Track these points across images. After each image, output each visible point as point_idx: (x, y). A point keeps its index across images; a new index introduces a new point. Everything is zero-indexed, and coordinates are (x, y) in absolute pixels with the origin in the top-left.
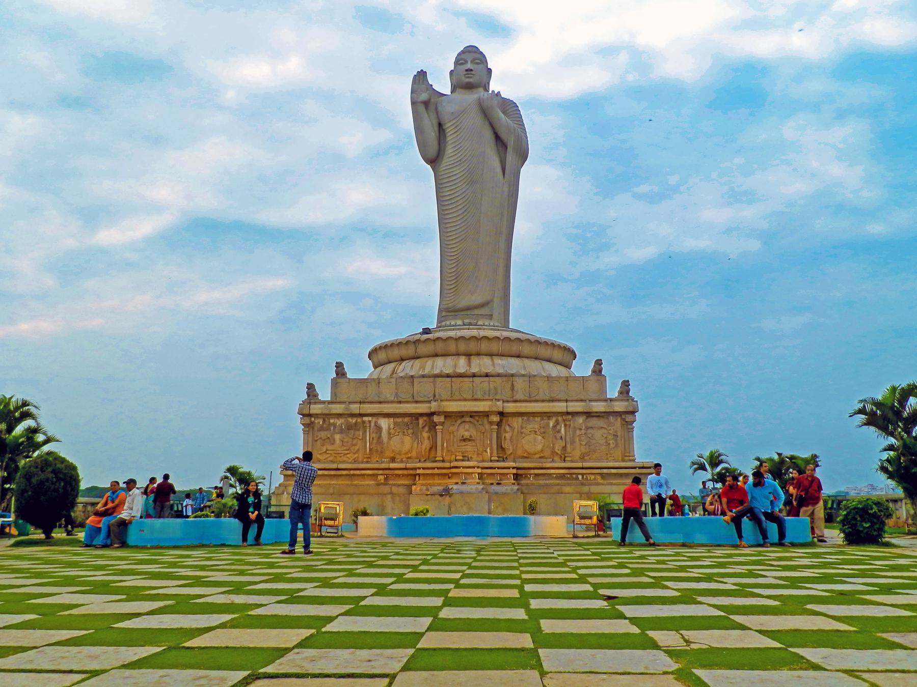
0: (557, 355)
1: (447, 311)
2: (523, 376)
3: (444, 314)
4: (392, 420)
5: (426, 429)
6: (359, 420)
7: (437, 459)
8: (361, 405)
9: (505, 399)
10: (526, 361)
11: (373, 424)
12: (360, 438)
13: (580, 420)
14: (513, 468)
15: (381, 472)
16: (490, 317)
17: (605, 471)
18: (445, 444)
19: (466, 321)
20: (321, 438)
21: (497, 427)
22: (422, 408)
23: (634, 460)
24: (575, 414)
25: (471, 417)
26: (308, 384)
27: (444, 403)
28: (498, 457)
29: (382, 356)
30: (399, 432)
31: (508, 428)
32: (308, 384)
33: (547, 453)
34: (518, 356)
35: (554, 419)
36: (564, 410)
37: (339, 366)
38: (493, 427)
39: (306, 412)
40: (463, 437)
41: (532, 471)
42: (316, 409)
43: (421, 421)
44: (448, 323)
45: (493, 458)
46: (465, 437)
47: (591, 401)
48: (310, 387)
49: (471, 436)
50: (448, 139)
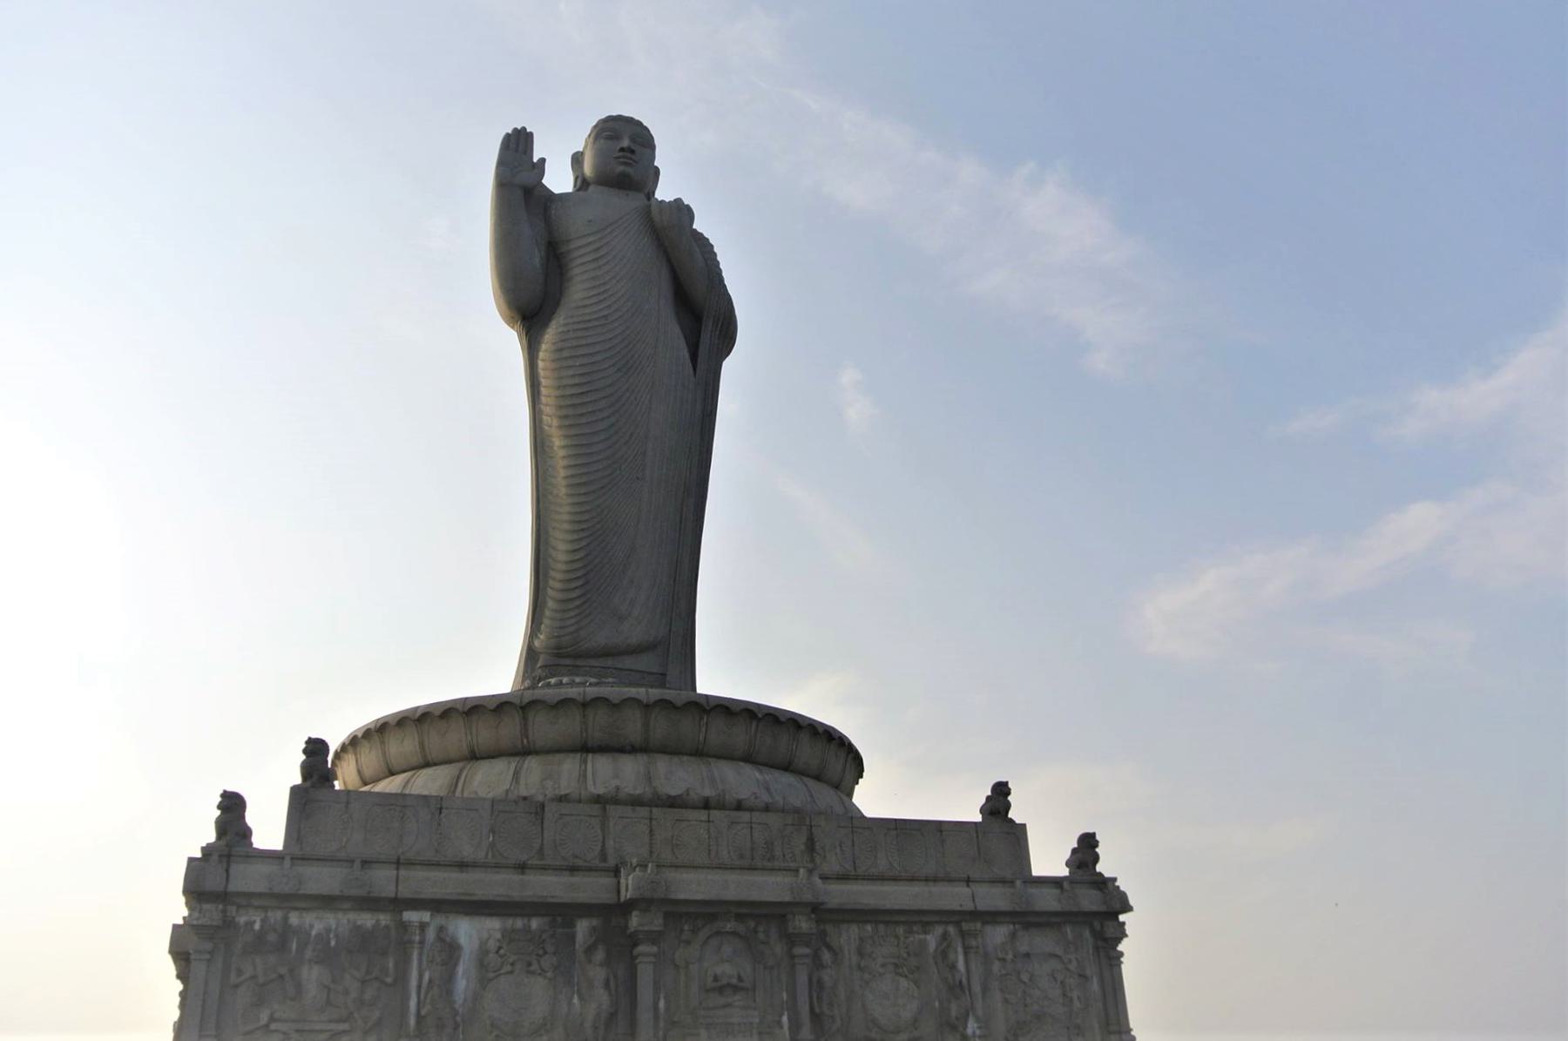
5: (600, 955)
8: (403, 872)
11: (431, 934)
12: (389, 980)
13: (997, 935)
20: (254, 977)
21: (807, 951)
22: (593, 889)
24: (992, 917)
27: (671, 875)
30: (512, 964)
31: (826, 956)
35: (939, 930)
36: (969, 906)
38: (799, 950)
39: (213, 883)
40: (716, 979)
42: (245, 879)
43: (583, 927)
46: (724, 981)
48: (232, 805)
50: (577, 271)
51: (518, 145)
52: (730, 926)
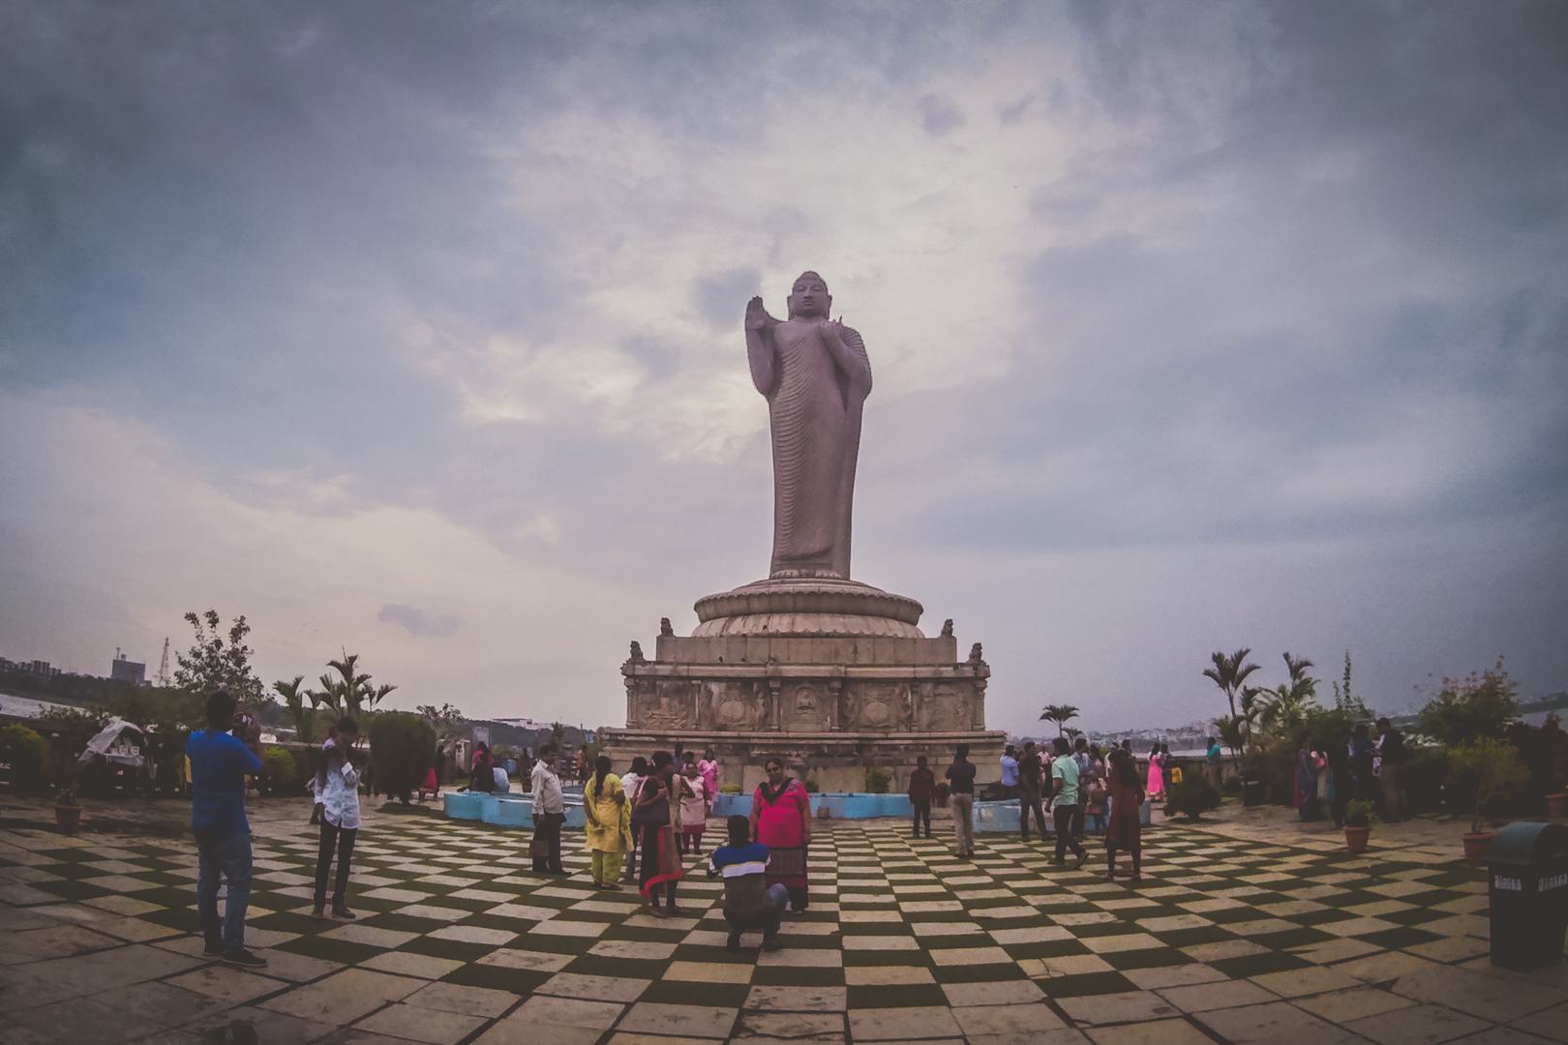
0: (904, 611)
1: (783, 560)
2: (868, 636)
3: (778, 562)
4: (724, 685)
7: (774, 727)
9: (848, 663)
10: (871, 620)
14: (856, 739)
16: (829, 567)
19: (804, 571)
22: (757, 672)
23: (983, 729)
24: (925, 680)
25: (811, 682)
26: (632, 642)
28: (839, 726)
29: (710, 610)
32: (632, 642)
33: (893, 721)
35: (901, 685)
37: (665, 622)
41: (876, 742)
42: (640, 670)
43: (755, 687)
44: (783, 572)
45: (833, 728)
47: (940, 665)
48: (635, 646)
49: (810, 704)
51: (756, 304)
52: (806, 685)
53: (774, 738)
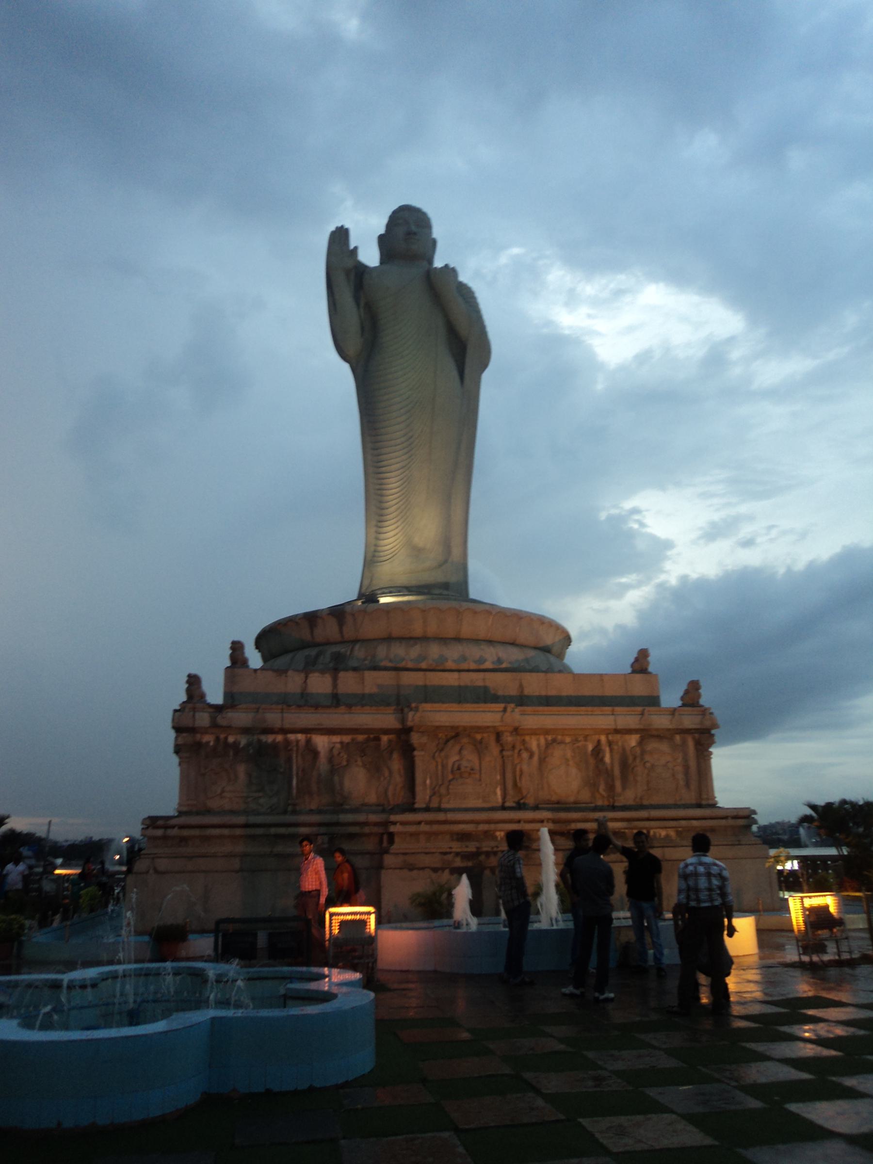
6: (279, 738)
7: (416, 806)
8: (285, 715)
15: (323, 830)
17: (683, 823)
18: (428, 782)
26: (190, 676)
32: (190, 676)
34: (513, 644)
39: (187, 722)
42: (203, 719)
45: (507, 804)
48: (193, 681)
51: (340, 236)
53: (430, 823)
